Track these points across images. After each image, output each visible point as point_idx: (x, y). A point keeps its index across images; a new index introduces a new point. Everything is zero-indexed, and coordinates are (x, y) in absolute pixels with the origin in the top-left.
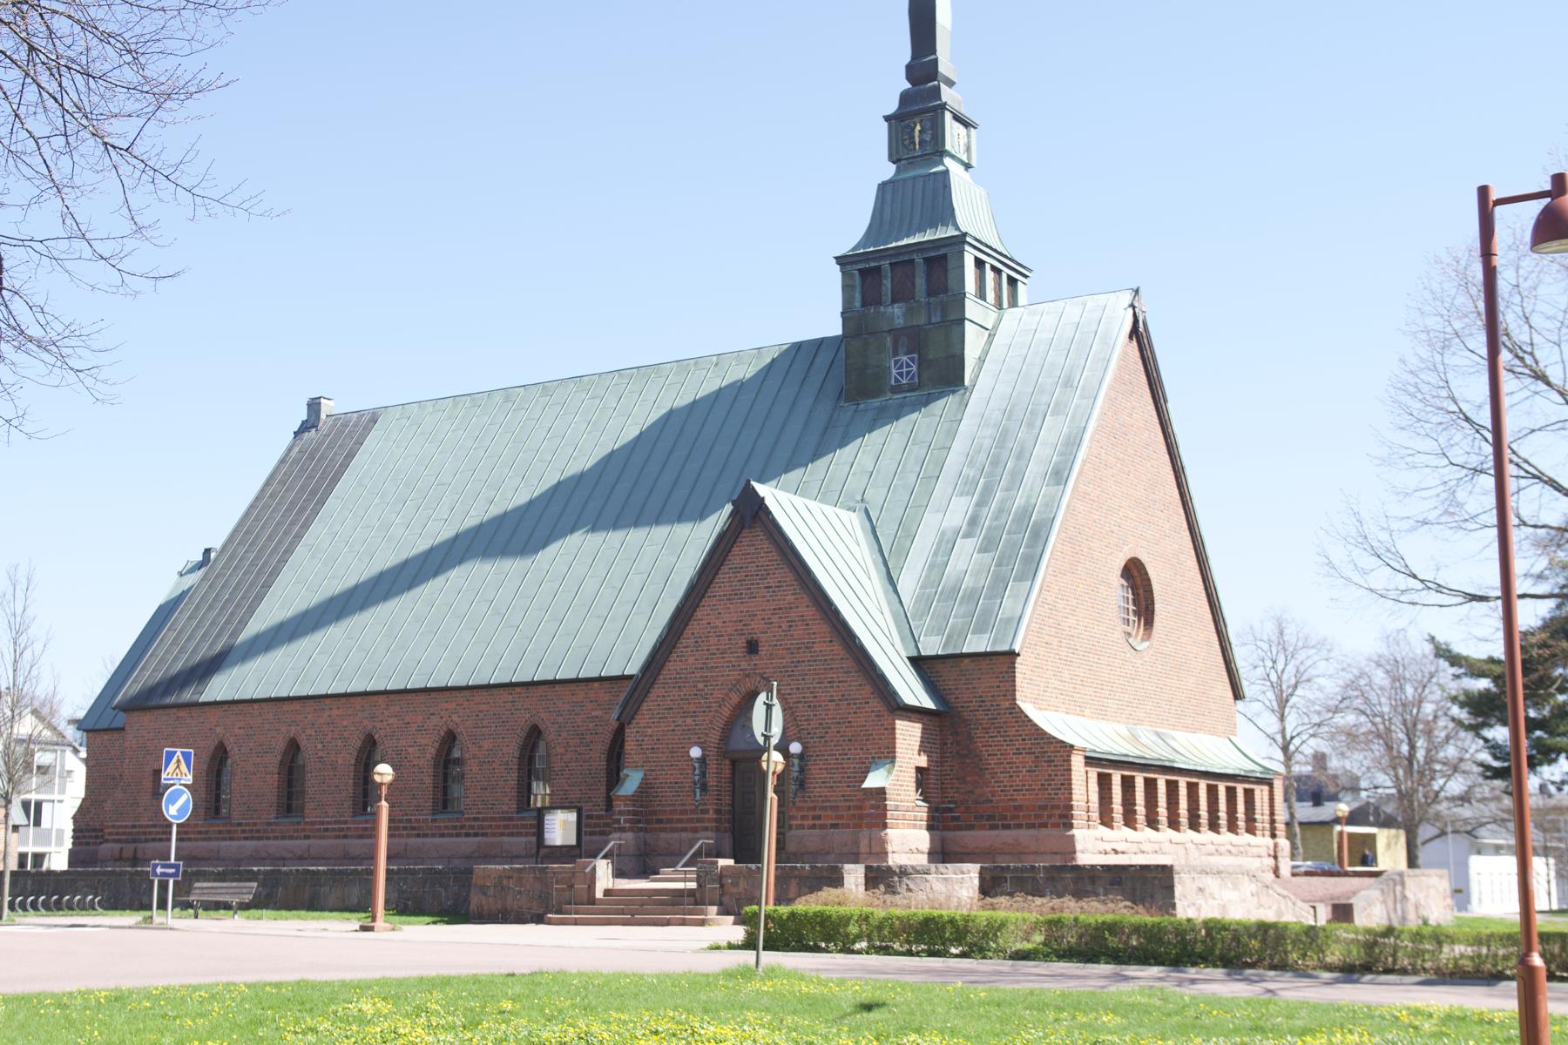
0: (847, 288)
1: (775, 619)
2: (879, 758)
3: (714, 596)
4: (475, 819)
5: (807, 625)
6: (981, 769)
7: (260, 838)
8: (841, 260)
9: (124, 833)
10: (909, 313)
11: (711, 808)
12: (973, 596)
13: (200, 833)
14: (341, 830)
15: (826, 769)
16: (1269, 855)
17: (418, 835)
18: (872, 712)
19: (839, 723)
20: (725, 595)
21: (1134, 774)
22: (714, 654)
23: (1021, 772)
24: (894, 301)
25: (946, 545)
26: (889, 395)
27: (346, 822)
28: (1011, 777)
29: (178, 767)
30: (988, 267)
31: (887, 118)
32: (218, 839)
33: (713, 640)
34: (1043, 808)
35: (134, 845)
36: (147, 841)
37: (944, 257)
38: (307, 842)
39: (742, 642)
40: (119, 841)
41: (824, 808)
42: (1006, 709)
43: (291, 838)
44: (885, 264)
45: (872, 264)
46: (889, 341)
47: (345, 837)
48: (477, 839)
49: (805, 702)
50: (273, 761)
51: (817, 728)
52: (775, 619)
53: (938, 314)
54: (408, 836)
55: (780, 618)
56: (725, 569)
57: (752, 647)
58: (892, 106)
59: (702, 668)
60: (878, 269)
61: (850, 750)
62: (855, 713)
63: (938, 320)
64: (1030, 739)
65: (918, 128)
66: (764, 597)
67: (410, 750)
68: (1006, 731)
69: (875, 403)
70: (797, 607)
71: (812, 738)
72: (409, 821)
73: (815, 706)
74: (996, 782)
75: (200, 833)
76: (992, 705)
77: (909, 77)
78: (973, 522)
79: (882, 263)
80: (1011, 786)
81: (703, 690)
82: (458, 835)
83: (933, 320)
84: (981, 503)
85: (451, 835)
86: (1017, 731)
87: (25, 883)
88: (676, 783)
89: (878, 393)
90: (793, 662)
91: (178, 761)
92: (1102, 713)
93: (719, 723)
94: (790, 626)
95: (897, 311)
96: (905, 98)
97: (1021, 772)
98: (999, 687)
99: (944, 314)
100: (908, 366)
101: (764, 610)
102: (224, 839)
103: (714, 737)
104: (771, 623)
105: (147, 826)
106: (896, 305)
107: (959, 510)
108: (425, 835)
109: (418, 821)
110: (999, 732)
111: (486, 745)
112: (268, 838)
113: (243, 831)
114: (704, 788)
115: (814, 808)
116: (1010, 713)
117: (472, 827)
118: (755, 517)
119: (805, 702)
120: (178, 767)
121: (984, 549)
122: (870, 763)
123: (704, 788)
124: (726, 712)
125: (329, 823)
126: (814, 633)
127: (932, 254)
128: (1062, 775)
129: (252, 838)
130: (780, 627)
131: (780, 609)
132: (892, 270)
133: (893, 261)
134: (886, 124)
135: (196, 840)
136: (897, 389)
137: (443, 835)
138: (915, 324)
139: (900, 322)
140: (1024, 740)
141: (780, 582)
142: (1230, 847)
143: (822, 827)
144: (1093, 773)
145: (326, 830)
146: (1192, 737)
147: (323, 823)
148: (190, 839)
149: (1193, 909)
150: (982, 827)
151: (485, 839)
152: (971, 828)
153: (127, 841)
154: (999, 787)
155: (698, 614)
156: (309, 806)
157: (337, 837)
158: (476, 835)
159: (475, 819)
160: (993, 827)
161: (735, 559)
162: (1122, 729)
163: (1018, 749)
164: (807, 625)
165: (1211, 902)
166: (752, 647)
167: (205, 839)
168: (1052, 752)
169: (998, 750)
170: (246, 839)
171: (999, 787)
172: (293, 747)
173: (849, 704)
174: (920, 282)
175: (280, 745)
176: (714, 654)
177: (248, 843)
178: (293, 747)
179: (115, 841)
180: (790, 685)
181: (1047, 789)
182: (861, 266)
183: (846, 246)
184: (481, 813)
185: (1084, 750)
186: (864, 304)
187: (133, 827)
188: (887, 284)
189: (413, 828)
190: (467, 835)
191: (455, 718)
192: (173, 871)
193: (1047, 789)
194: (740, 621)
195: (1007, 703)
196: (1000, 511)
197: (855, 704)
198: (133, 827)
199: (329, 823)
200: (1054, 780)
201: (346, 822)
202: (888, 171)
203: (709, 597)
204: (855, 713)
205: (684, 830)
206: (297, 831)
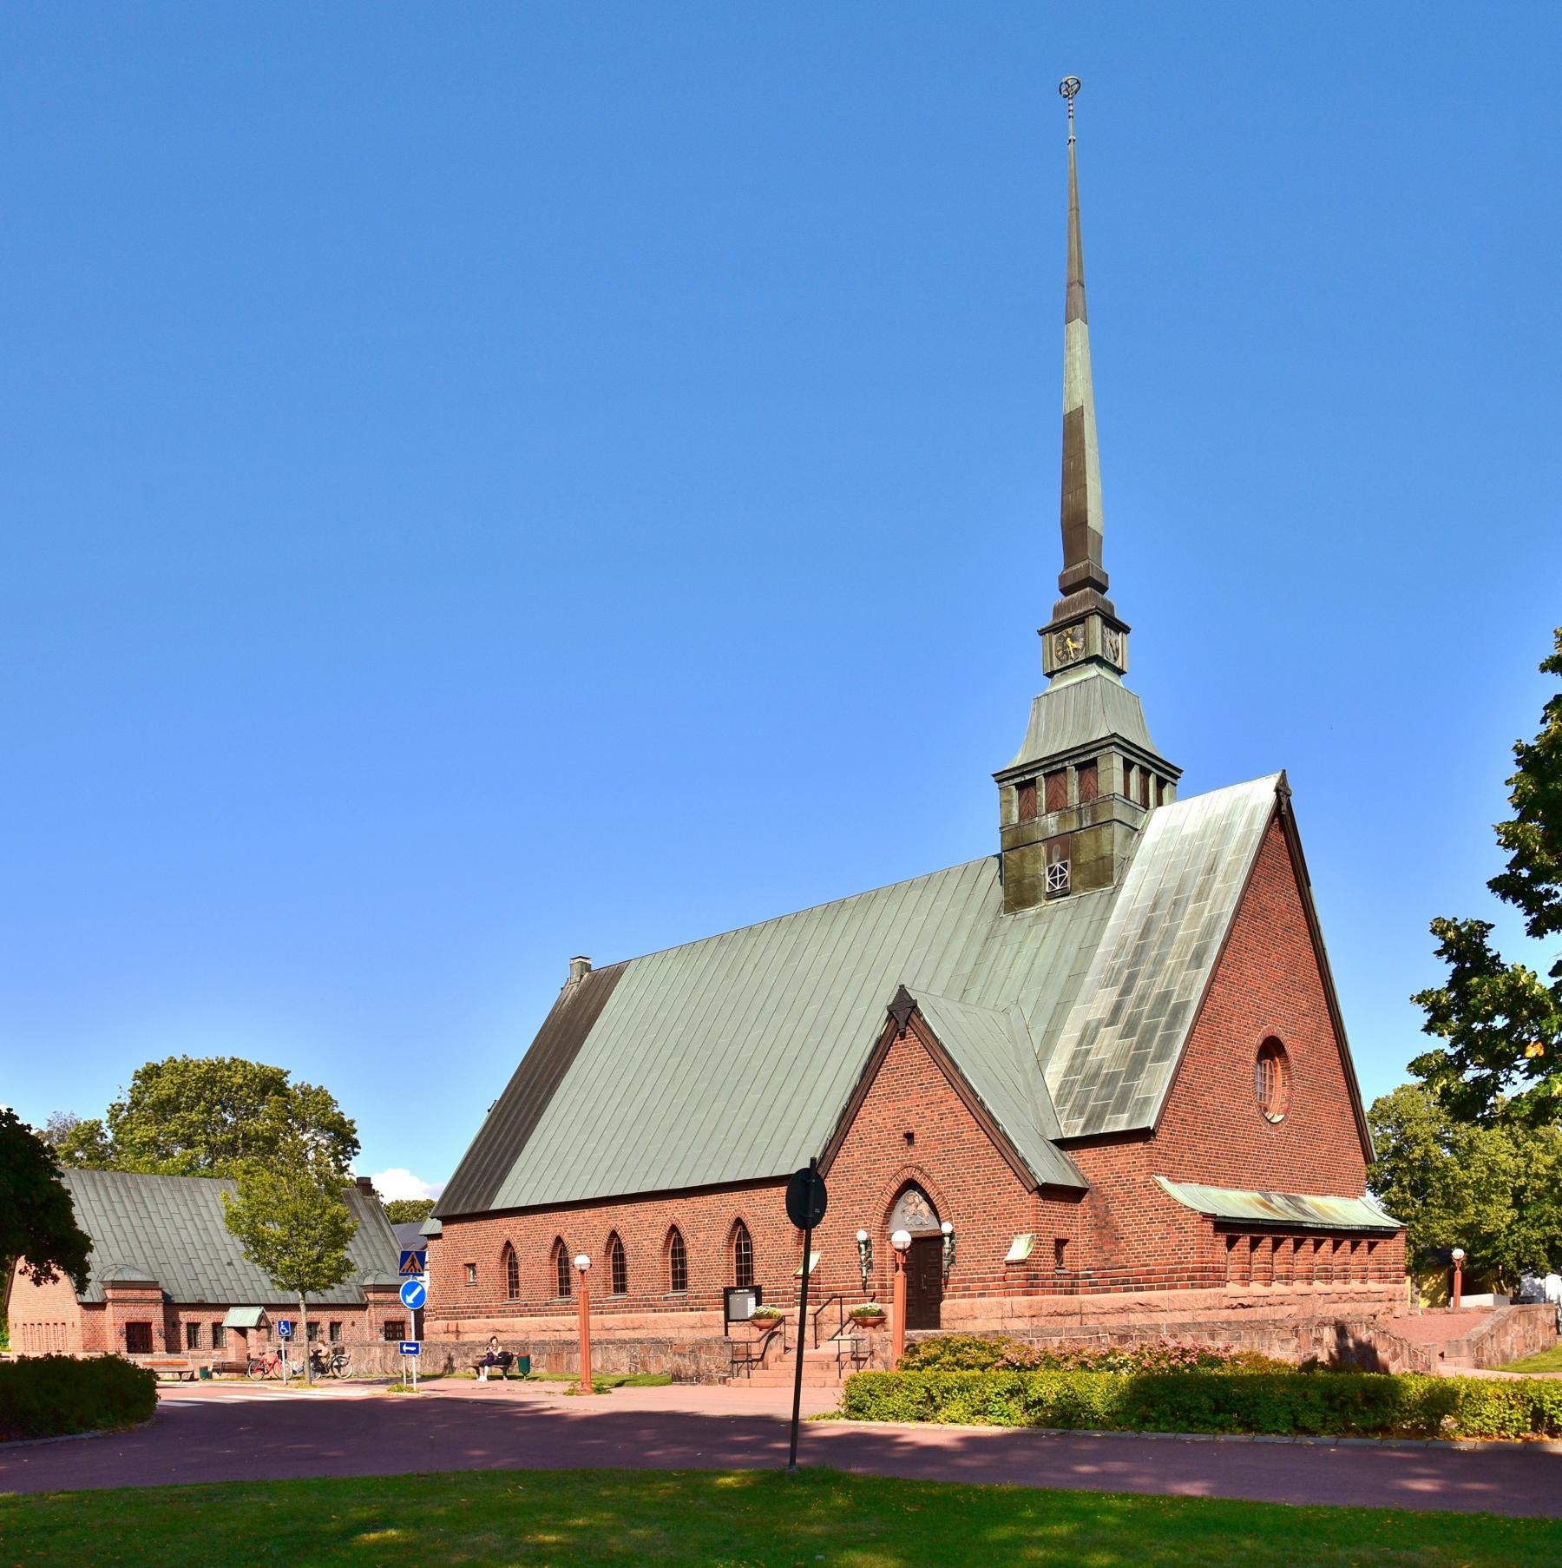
2: (1021, 1233)
3: (874, 1096)
4: (697, 1297)
5: (956, 1116)
6: (1117, 1239)
9: (449, 1313)
10: (1063, 819)
12: (1112, 1079)
13: (500, 1312)
15: (974, 1245)
17: (655, 1311)
18: (1015, 1192)
19: (985, 1204)
20: (884, 1095)
22: (876, 1148)
23: (1154, 1239)
24: (1048, 811)
25: (1088, 1035)
26: (1044, 902)
27: (600, 1302)
28: (1144, 1244)
29: (413, 1264)
32: (512, 1317)
33: (875, 1135)
34: (1173, 1271)
35: (456, 1321)
36: (464, 1318)
39: (899, 1135)
40: (446, 1319)
42: (1141, 1183)
45: (1028, 777)
46: (1043, 850)
47: (601, 1313)
48: (700, 1312)
49: (955, 1187)
51: (966, 1210)
53: (1089, 818)
54: (648, 1312)
55: (932, 1111)
57: (909, 1137)
59: (866, 1162)
61: (995, 1227)
62: (1000, 1194)
63: (1089, 824)
64: (1162, 1209)
66: (917, 1093)
68: (1141, 1203)
70: (948, 1101)
71: (962, 1218)
72: (648, 1300)
73: (963, 1190)
74: (1130, 1250)
75: (500, 1312)
76: (1128, 1180)
78: (1117, 1009)
79: (1036, 774)
80: (1144, 1252)
81: (867, 1181)
82: (684, 1310)
83: (1084, 825)
84: (1125, 991)
85: (679, 1310)
86: (1151, 1202)
87: (376, 1352)
88: (847, 1263)
90: (944, 1151)
91: (413, 1260)
94: (941, 1119)
97: (1154, 1239)
98: (1134, 1162)
99: (1093, 819)
101: (918, 1106)
102: (517, 1316)
104: (925, 1117)
105: (464, 1308)
106: (1049, 815)
107: (1107, 998)
108: (660, 1311)
109: (654, 1300)
110: (1134, 1204)
111: (702, 1236)
112: (547, 1315)
113: (529, 1310)
115: (963, 1281)
116: (1144, 1187)
117: (695, 1304)
119: (955, 1187)
120: (413, 1264)
121: (1125, 1035)
122: (1013, 1238)
126: (962, 1124)
128: (1192, 1240)
130: (932, 1120)
131: (932, 1103)
132: (1046, 782)
133: (1046, 771)
135: (497, 1317)
137: (673, 1310)
138: (1068, 830)
139: (1053, 831)
140: (1157, 1210)
141: (932, 1078)
143: (971, 1296)
148: (493, 1317)
151: (704, 1313)
153: (451, 1319)
154: (1133, 1253)
155: (861, 1113)
158: (698, 1310)
159: (697, 1297)
163: (1151, 1219)
164: (956, 1116)
166: (909, 1137)
167: (503, 1317)
168: (1183, 1220)
169: (1133, 1221)
171: (1133, 1253)
173: (994, 1186)
176: (876, 1148)
177: (534, 1318)
179: (443, 1319)
180: (942, 1172)
181: (1178, 1254)
182: (1017, 780)
184: (701, 1292)
186: (1021, 817)
189: (651, 1306)
190: (692, 1310)
192: (413, 1349)
193: (1178, 1254)
194: (898, 1117)
195: (1142, 1177)
196: (1142, 998)
197: (999, 1186)
198: (455, 1308)
200: (1184, 1245)
201: (600, 1302)
203: (871, 1097)
204: (1000, 1194)
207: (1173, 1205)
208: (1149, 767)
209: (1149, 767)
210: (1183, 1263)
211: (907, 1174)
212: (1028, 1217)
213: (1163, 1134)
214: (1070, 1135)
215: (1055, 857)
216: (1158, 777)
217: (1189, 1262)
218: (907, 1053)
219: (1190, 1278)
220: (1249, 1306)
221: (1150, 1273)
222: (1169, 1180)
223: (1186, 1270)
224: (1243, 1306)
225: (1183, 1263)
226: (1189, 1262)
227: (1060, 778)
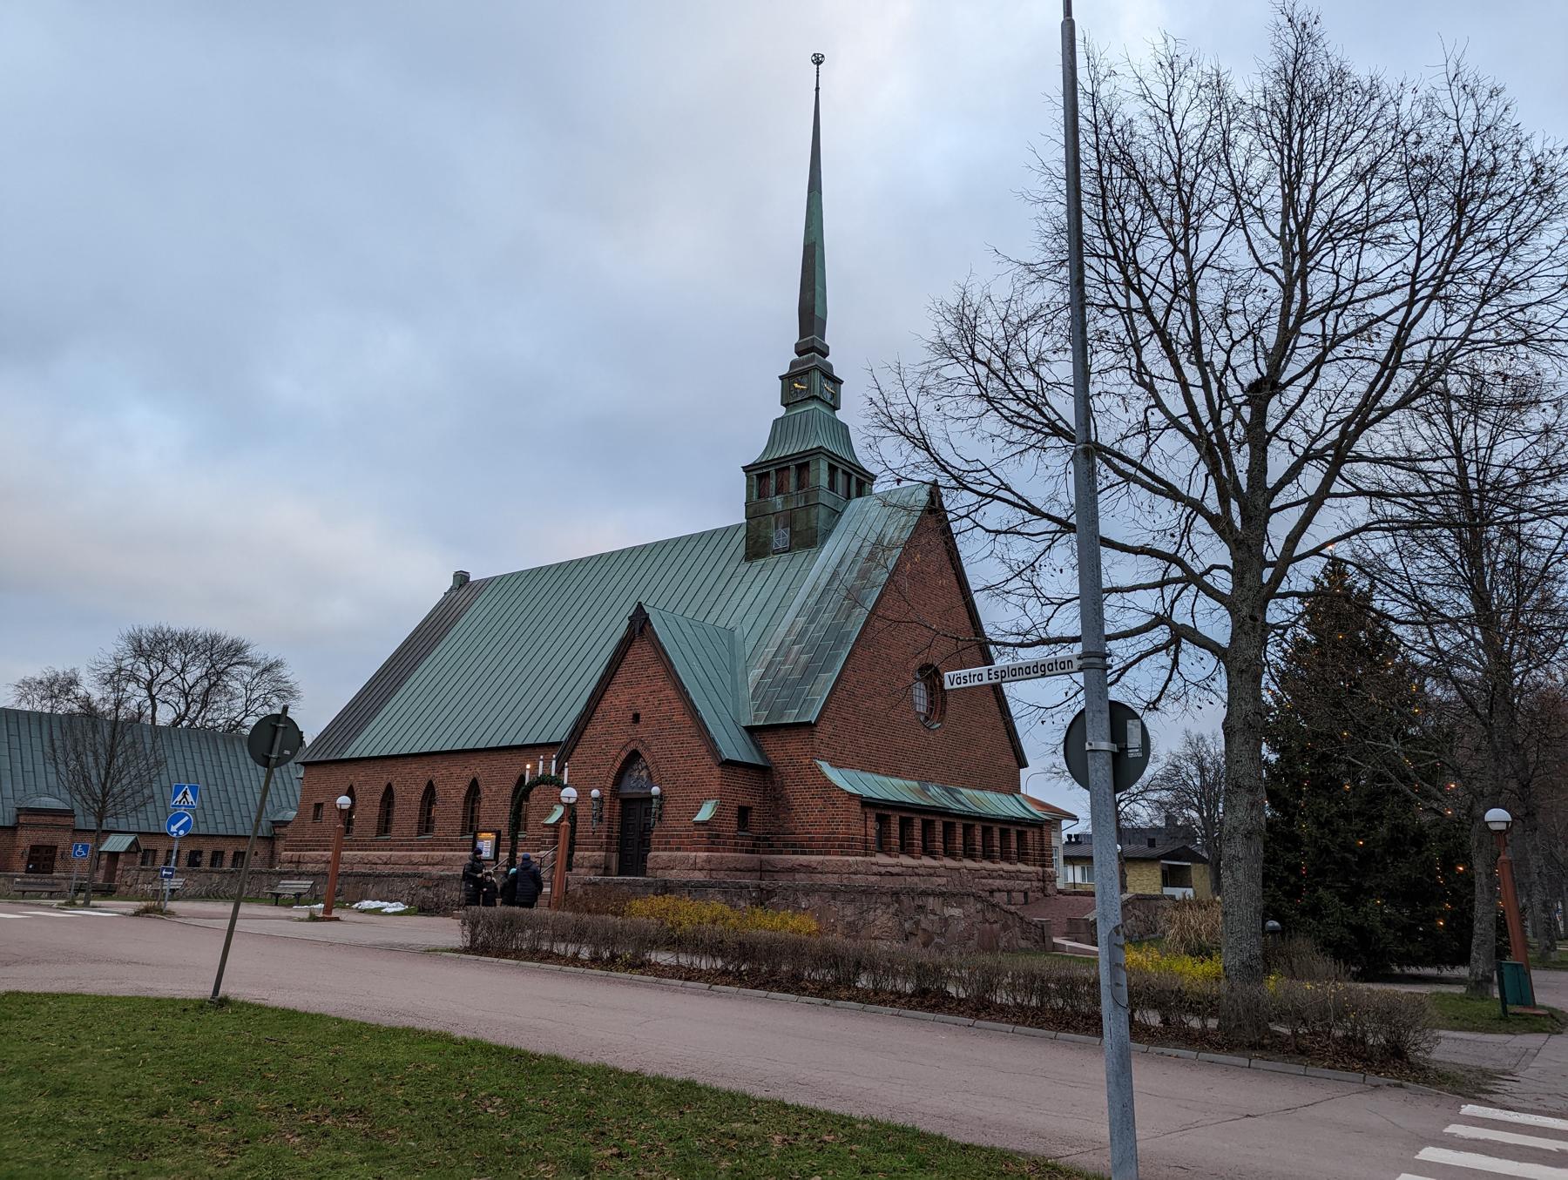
0: (749, 487)
1: (651, 698)
7: (366, 850)
8: (747, 469)
10: (786, 501)
11: (604, 835)
14: (410, 845)
16: (1039, 880)
17: (451, 850)
21: (934, 818)
24: (776, 494)
27: (412, 840)
29: (185, 797)
30: (840, 471)
31: (781, 378)
34: (827, 840)
37: (807, 464)
38: (390, 853)
39: (630, 715)
41: (672, 836)
43: (383, 850)
44: (772, 470)
50: (378, 797)
52: (651, 698)
56: (623, 665)
57: (636, 718)
58: (785, 370)
60: (768, 473)
65: (796, 385)
67: (452, 792)
69: (762, 561)
77: (799, 353)
89: (764, 555)
92: (896, 773)
93: (613, 774)
95: (779, 500)
96: (793, 364)
99: (806, 501)
100: (784, 536)
103: (610, 781)
108: (455, 850)
109: (452, 840)
114: (601, 819)
118: (641, 630)
120: (185, 797)
123: (601, 819)
124: (618, 765)
125: (404, 840)
127: (801, 462)
129: (362, 850)
134: (780, 382)
136: (776, 552)
139: (780, 507)
142: (1001, 873)
144: (872, 816)
145: (402, 845)
146: (977, 793)
147: (400, 840)
149: (911, 922)
150: (788, 853)
152: (781, 853)
156: (394, 829)
157: (407, 850)
160: (795, 853)
161: (630, 658)
162: (915, 784)
165: (931, 917)
166: (636, 718)
170: (359, 850)
172: (389, 788)
174: (793, 480)
175: (383, 788)
178: (389, 788)
182: (758, 472)
183: (753, 456)
185: (861, 796)
187: (301, 841)
188: (773, 482)
189: (449, 845)
191: (478, 770)
199: (404, 840)
201: (412, 840)
202: (781, 411)
205: (587, 850)
206: (386, 845)
207: (829, 785)
208: (851, 471)
209: (851, 471)
210: (834, 833)
211: (632, 746)
212: (715, 785)
213: (826, 728)
214: (757, 724)
215: (780, 526)
216: (857, 479)
217: (839, 833)
218: (641, 651)
219: (841, 846)
220: (898, 874)
221: (811, 839)
222: (831, 766)
223: (837, 839)
224: (892, 874)
225: (834, 833)
226: (839, 833)
227: (786, 473)
